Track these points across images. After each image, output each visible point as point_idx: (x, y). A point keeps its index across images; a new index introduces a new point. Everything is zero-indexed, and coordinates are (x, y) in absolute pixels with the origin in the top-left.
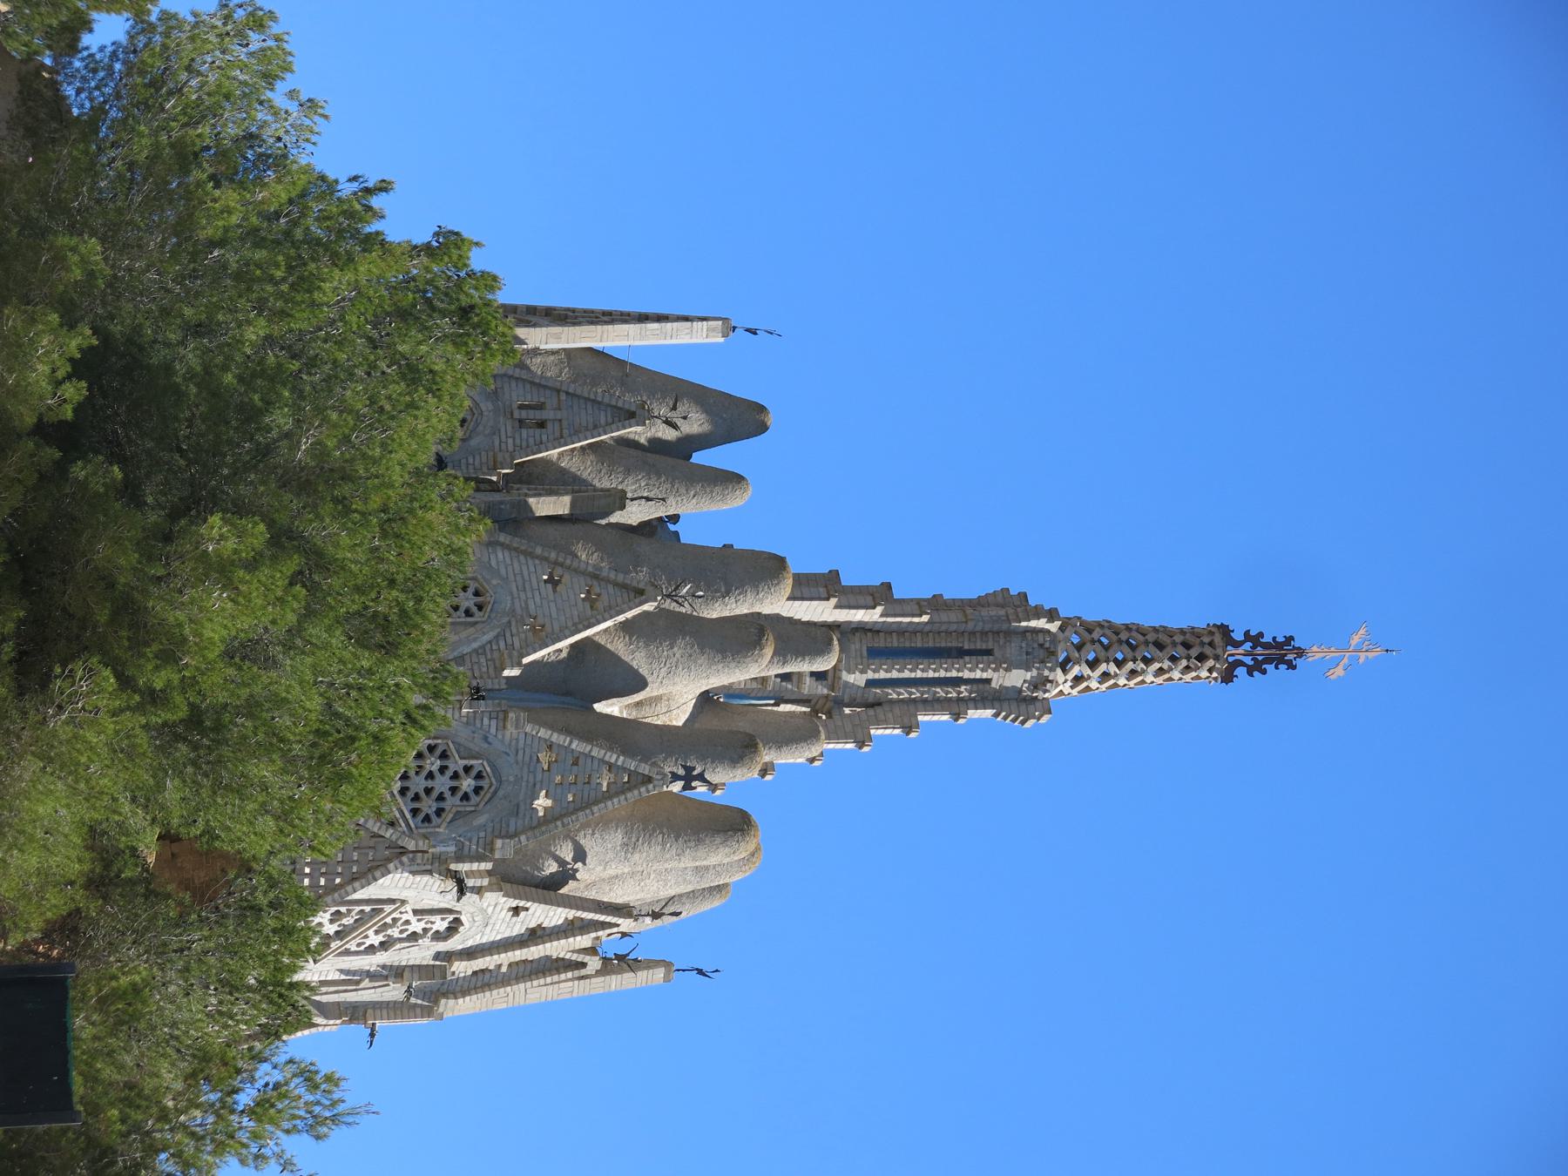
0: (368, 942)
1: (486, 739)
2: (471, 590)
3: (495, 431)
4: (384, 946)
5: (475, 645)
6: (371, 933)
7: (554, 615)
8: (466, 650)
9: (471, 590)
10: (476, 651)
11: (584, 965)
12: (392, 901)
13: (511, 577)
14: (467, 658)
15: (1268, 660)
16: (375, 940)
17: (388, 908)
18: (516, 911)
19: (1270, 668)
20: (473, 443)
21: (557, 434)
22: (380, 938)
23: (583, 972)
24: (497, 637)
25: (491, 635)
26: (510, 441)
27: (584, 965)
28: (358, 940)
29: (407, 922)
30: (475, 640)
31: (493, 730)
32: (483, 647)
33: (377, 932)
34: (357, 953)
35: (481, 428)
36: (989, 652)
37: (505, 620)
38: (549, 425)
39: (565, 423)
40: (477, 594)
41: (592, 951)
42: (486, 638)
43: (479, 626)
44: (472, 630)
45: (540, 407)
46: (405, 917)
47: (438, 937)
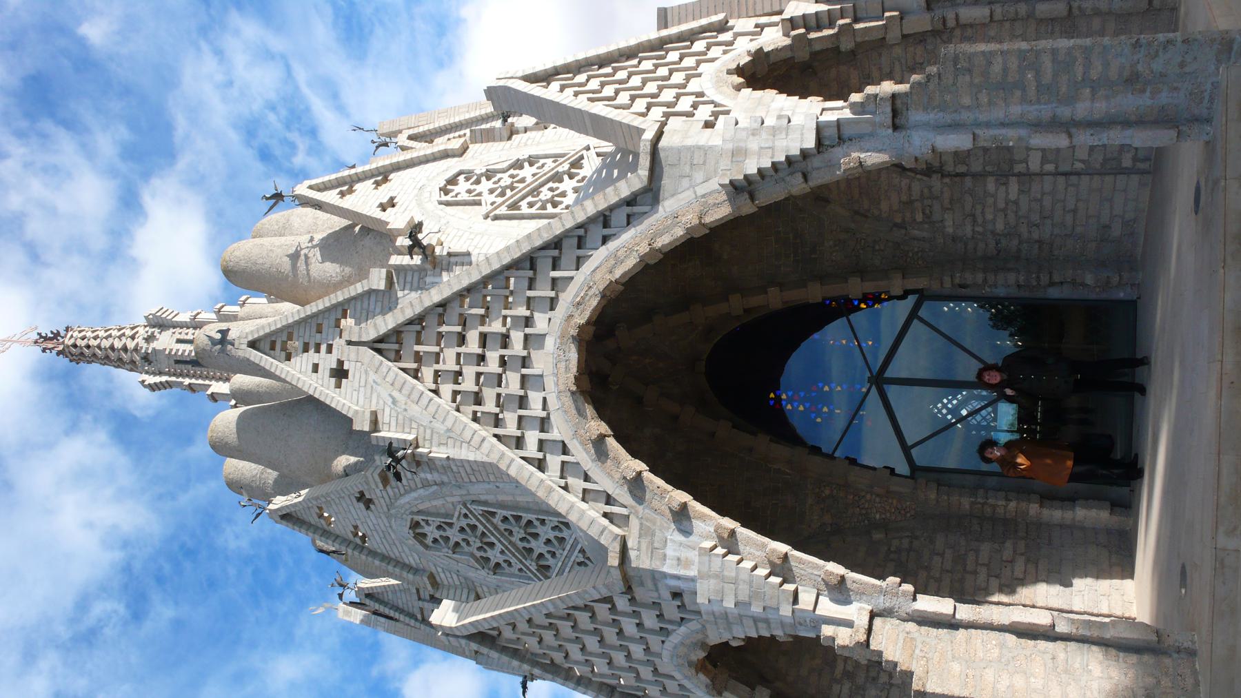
0: (534, 169)
1: (394, 402)
4: (518, 165)
5: (414, 495)
6: (529, 179)
8: (421, 491)
10: (412, 490)
11: (411, 138)
12: (496, 218)
14: (420, 485)
15: (51, 339)
16: (527, 172)
17: (503, 210)
18: (391, 203)
19: (50, 335)
22: (521, 174)
23: (411, 132)
24: (396, 499)
27: (411, 138)
28: (546, 169)
29: (491, 191)
30: (416, 499)
31: (387, 410)
32: (407, 492)
33: (523, 180)
34: (546, 157)
36: (177, 362)
37: (393, 511)
41: (403, 148)
42: (406, 499)
43: (415, 510)
44: (421, 507)
46: (492, 198)
47: (468, 174)
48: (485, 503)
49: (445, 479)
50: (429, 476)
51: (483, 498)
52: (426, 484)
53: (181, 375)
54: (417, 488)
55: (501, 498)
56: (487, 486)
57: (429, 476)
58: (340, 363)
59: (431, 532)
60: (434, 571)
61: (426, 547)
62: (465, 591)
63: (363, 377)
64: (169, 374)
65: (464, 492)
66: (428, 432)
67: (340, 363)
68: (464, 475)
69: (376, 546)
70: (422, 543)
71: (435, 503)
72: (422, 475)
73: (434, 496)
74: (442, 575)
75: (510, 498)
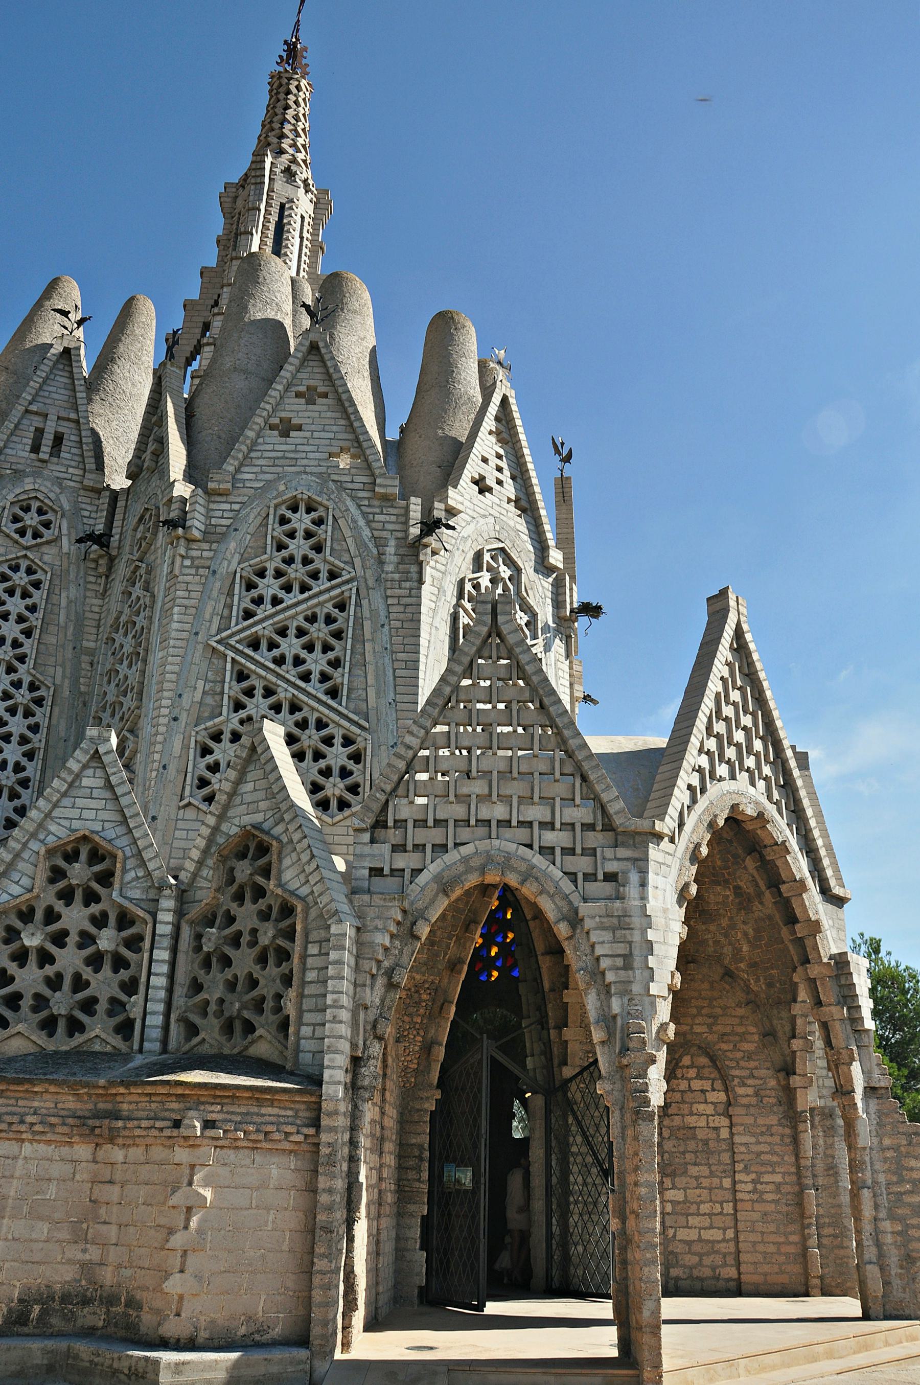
2: (289, 514)
3: (59, 481)
5: (361, 522)
7: (331, 435)
8: (366, 533)
9: (289, 514)
10: (368, 523)
13: (280, 469)
20: (66, 506)
21: (72, 425)
24: (353, 498)
25: (349, 502)
26: (71, 470)
30: (355, 521)
32: (364, 515)
35: (51, 495)
38: (60, 429)
39: (63, 414)
40: (295, 509)
45: (40, 432)
48: (358, 604)
49: (389, 568)
50: (390, 550)
51: (365, 603)
52: (380, 543)
53: (268, 204)
54: (372, 529)
55: (367, 625)
56: (383, 613)
57: (390, 550)
58: (490, 490)
59: (302, 521)
60: (231, 498)
61: (276, 507)
62: (203, 528)
63: (482, 512)
64: (271, 190)
65: (371, 583)
66: (443, 568)
67: (490, 490)
68: (398, 592)
69: (268, 440)
70: (284, 502)
71: (350, 541)
72: (392, 543)
73: (361, 544)
74: (226, 506)
75: (367, 636)
